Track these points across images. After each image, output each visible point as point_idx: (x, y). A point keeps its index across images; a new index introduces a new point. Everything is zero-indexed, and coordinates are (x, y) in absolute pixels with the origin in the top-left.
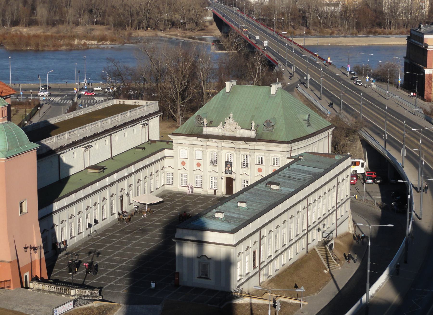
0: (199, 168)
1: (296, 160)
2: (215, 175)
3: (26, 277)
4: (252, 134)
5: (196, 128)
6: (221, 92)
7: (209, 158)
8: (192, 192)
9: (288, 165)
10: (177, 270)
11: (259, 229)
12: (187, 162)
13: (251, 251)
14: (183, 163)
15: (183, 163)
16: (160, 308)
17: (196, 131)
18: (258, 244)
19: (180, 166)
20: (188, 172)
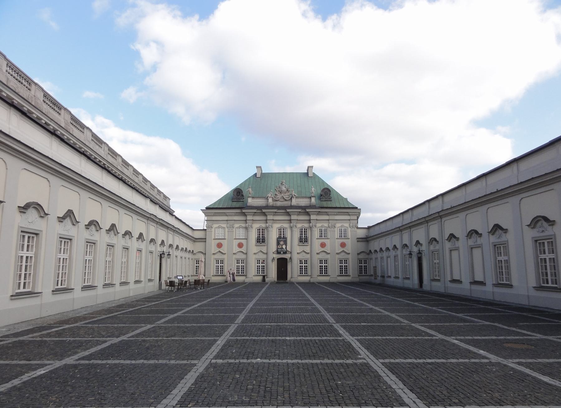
0: (241, 250)
2: (262, 256)
5: (235, 203)
7: (253, 235)
8: (234, 280)
14: (220, 245)
15: (220, 245)
19: (214, 249)
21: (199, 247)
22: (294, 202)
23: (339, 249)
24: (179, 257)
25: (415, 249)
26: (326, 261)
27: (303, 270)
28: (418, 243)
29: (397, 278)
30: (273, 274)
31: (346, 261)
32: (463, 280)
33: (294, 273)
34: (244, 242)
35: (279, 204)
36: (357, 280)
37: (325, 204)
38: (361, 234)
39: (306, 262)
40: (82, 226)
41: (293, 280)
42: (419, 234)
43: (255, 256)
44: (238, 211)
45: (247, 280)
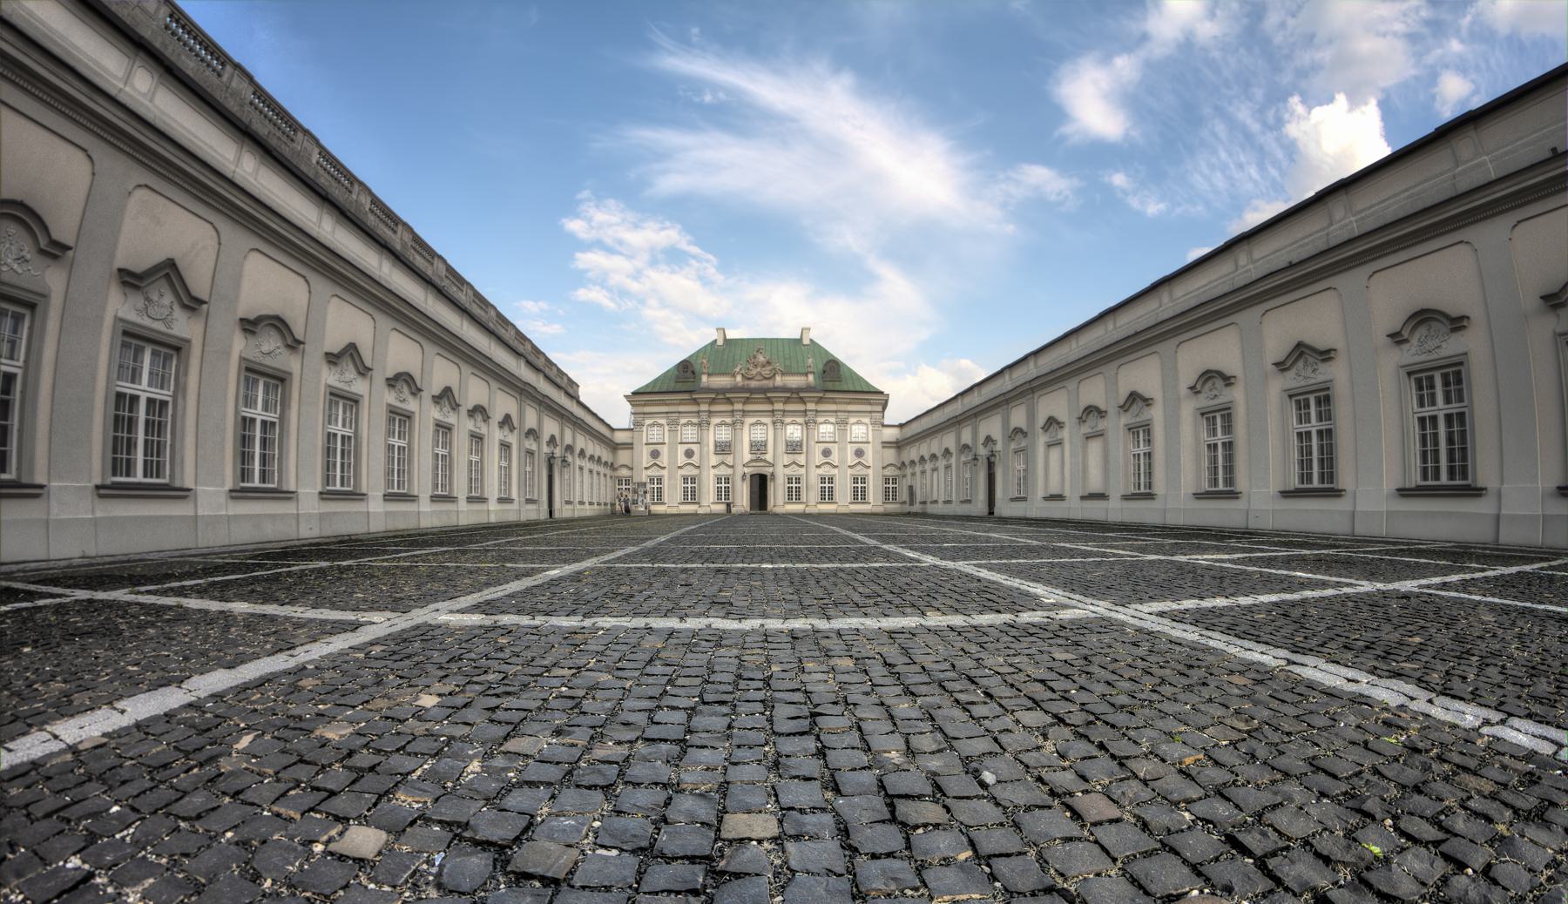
2: (724, 471)
12: (664, 450)
14: (655, 454)
15: (655, 454)
19: (646, 460)
20: (665, 473)
22: (779, 381)
23: (851, 459)
24: (586, 472)
25: (983, 452)
26: (831, 480)
27: (794, 494)
28: (989, 439)
29: (948, 502)
30: (742, 499)
31: (864, 480)
32: (1067, 493)
33: (778, 501)
34: (695, 448)
35: (753, 384)
36: (880, 510)
37: (830, 386)
38: (891, 434)
39: (798, 480)
40: (379, 378)
41: (779, 510)
42: (992, 426)
43: (713, 472)
44: (686, 396)
45: (701, 511)
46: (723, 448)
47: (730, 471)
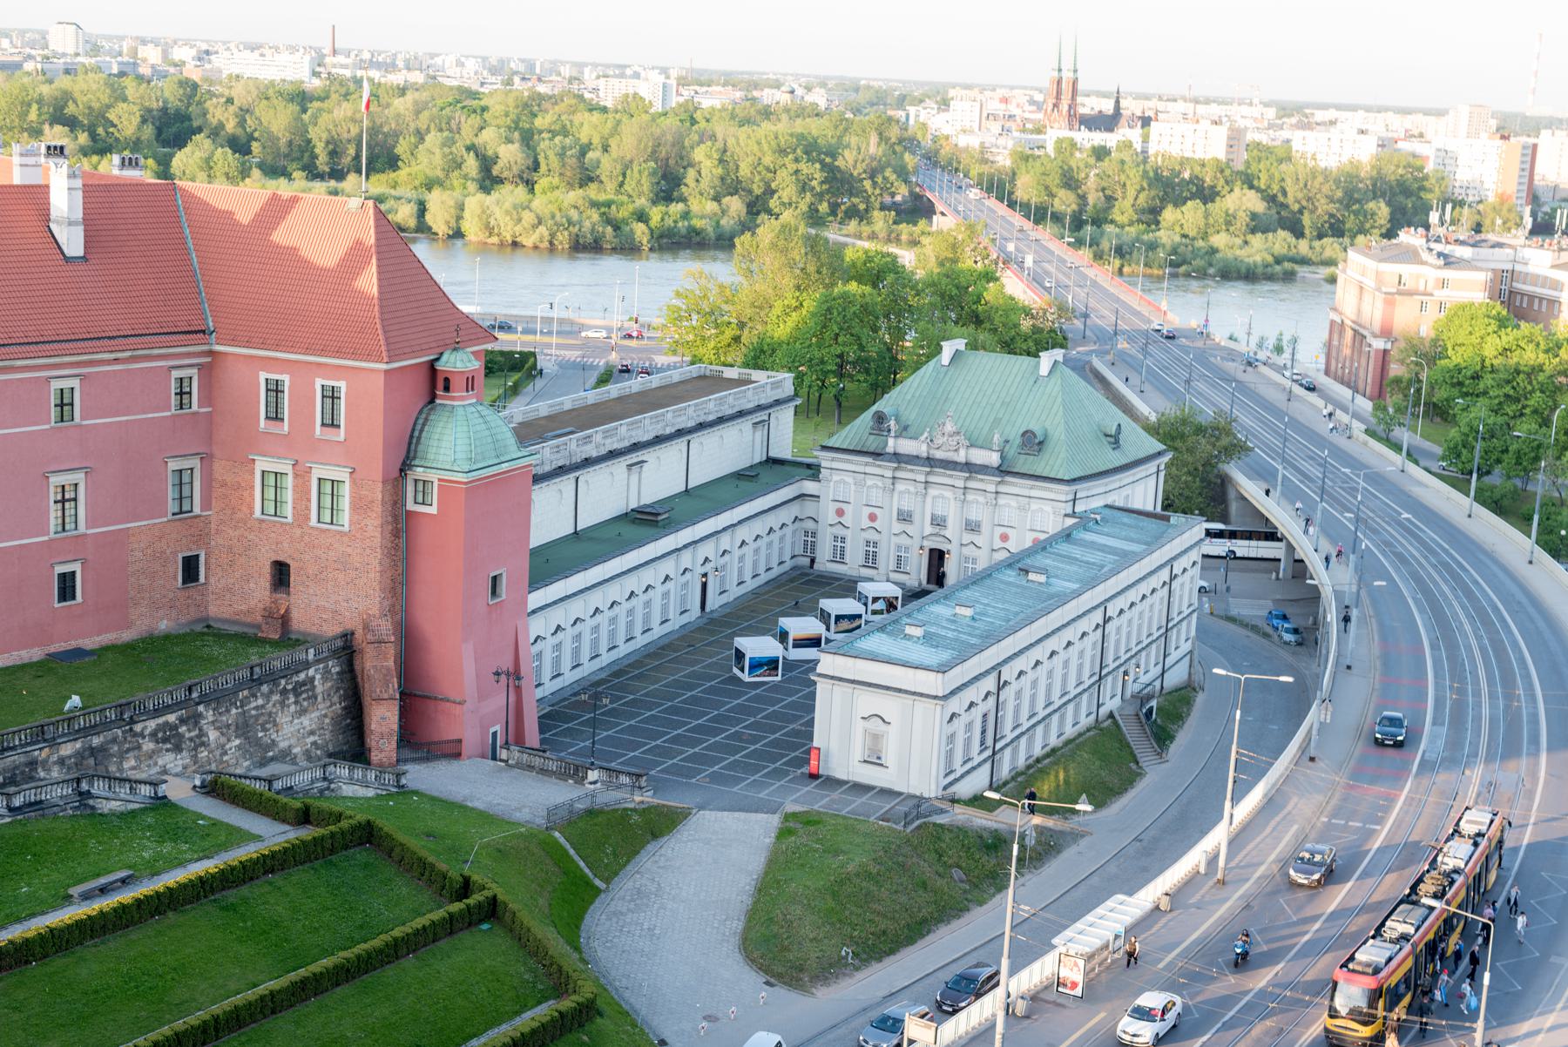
1: (1084, 521)
2: (904, 540)
3: (495, 734)
4: (993, 459)
6: (932, 363)
9: (1067, 536)
10: (815, 744)
11: (997, 668)
13: (977, 714)
14: (840, 513)
15: (840, 513)
16: (775, 820)
17: (873, 443)
18: (992, 700)
19: (832, 518)
20: (848, 533)
21: (809, 508)
22: (961, 457)
35: (939, 455)
44: (870, 460)
46: (905, 517)
47: (907, 541)
